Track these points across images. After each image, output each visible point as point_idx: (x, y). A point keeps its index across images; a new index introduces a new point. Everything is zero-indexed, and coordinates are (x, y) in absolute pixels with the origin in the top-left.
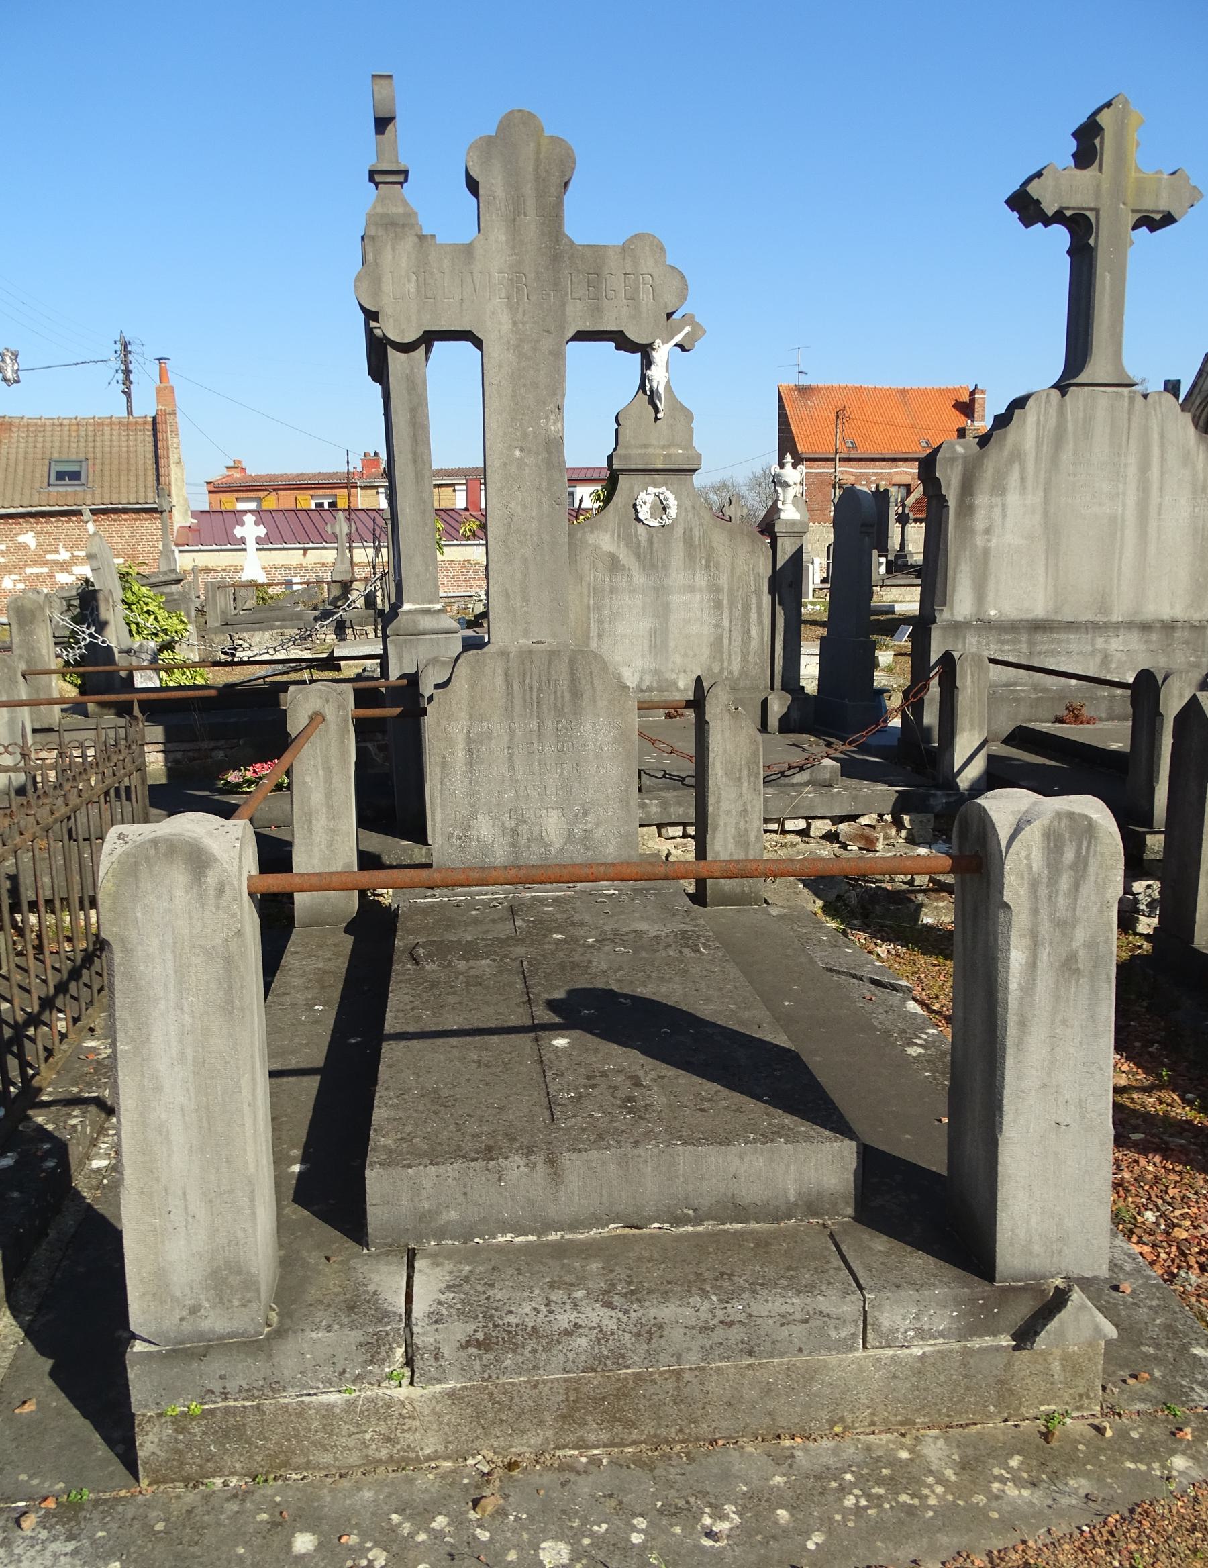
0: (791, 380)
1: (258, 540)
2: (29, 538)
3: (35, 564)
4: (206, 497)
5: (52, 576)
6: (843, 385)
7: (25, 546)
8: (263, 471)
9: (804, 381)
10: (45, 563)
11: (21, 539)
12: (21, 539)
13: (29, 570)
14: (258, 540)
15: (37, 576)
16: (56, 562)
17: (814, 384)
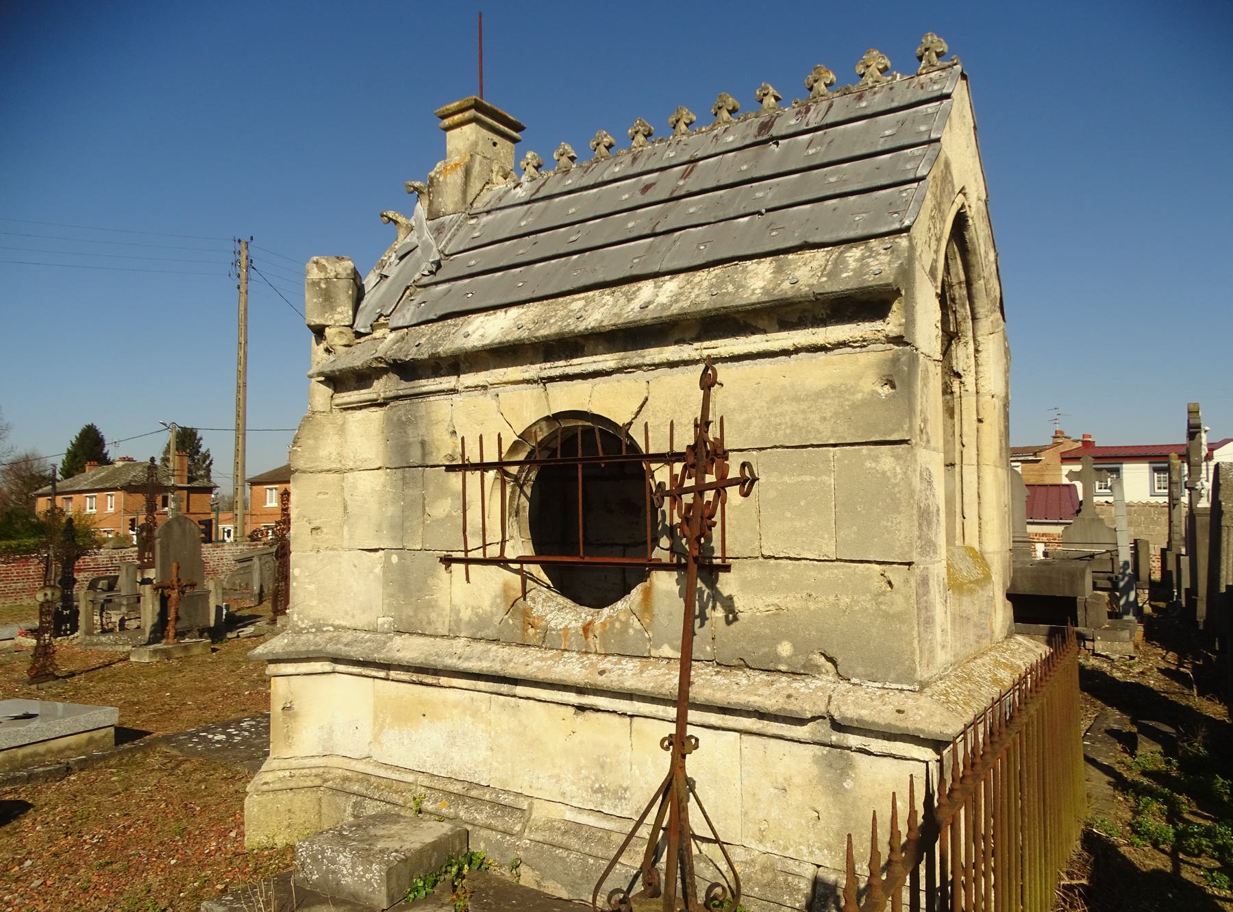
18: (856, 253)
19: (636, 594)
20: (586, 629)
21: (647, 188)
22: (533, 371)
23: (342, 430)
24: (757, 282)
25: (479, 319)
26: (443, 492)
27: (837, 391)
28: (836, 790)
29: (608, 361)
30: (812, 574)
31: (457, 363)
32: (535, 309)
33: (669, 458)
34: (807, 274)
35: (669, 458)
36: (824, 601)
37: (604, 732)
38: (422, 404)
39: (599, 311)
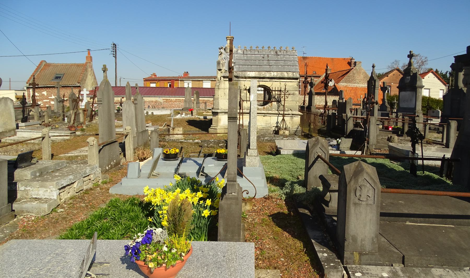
0: (302, 55)
1: (87, 95)
2: (45, 93)
3: (46, 99)
4: (143, 82)
5: (50, 102)
6: (316, 57)
7: (44, 95)
8: (160, 76)
9: (305, 56)
10: (48, 99)
11: (43, 93)
12: (43, 93)
13: (44, 101)
14: (87, 95)
15: (46, 102)
16: (51, 99)
17: (307, 56)
18: (294, 73)
19: (270, 104)
20: (264, 108)
21: (263, 57)
22: (258, 80)
23: (224, 83)
24: (286, 75)
25: (248, 73)
26: (243, 93)
27: (293, 86)
28: (292, 120)
29: (268, 80)
30: (290, 102)
31: (246, 78)
32: (257, 73)
33: (275, 91)
34: (291, 75)
35: (275, 91)
36: (290, 104)
37: (267, 118)
38: (239, 82)
39: (268, 75)
